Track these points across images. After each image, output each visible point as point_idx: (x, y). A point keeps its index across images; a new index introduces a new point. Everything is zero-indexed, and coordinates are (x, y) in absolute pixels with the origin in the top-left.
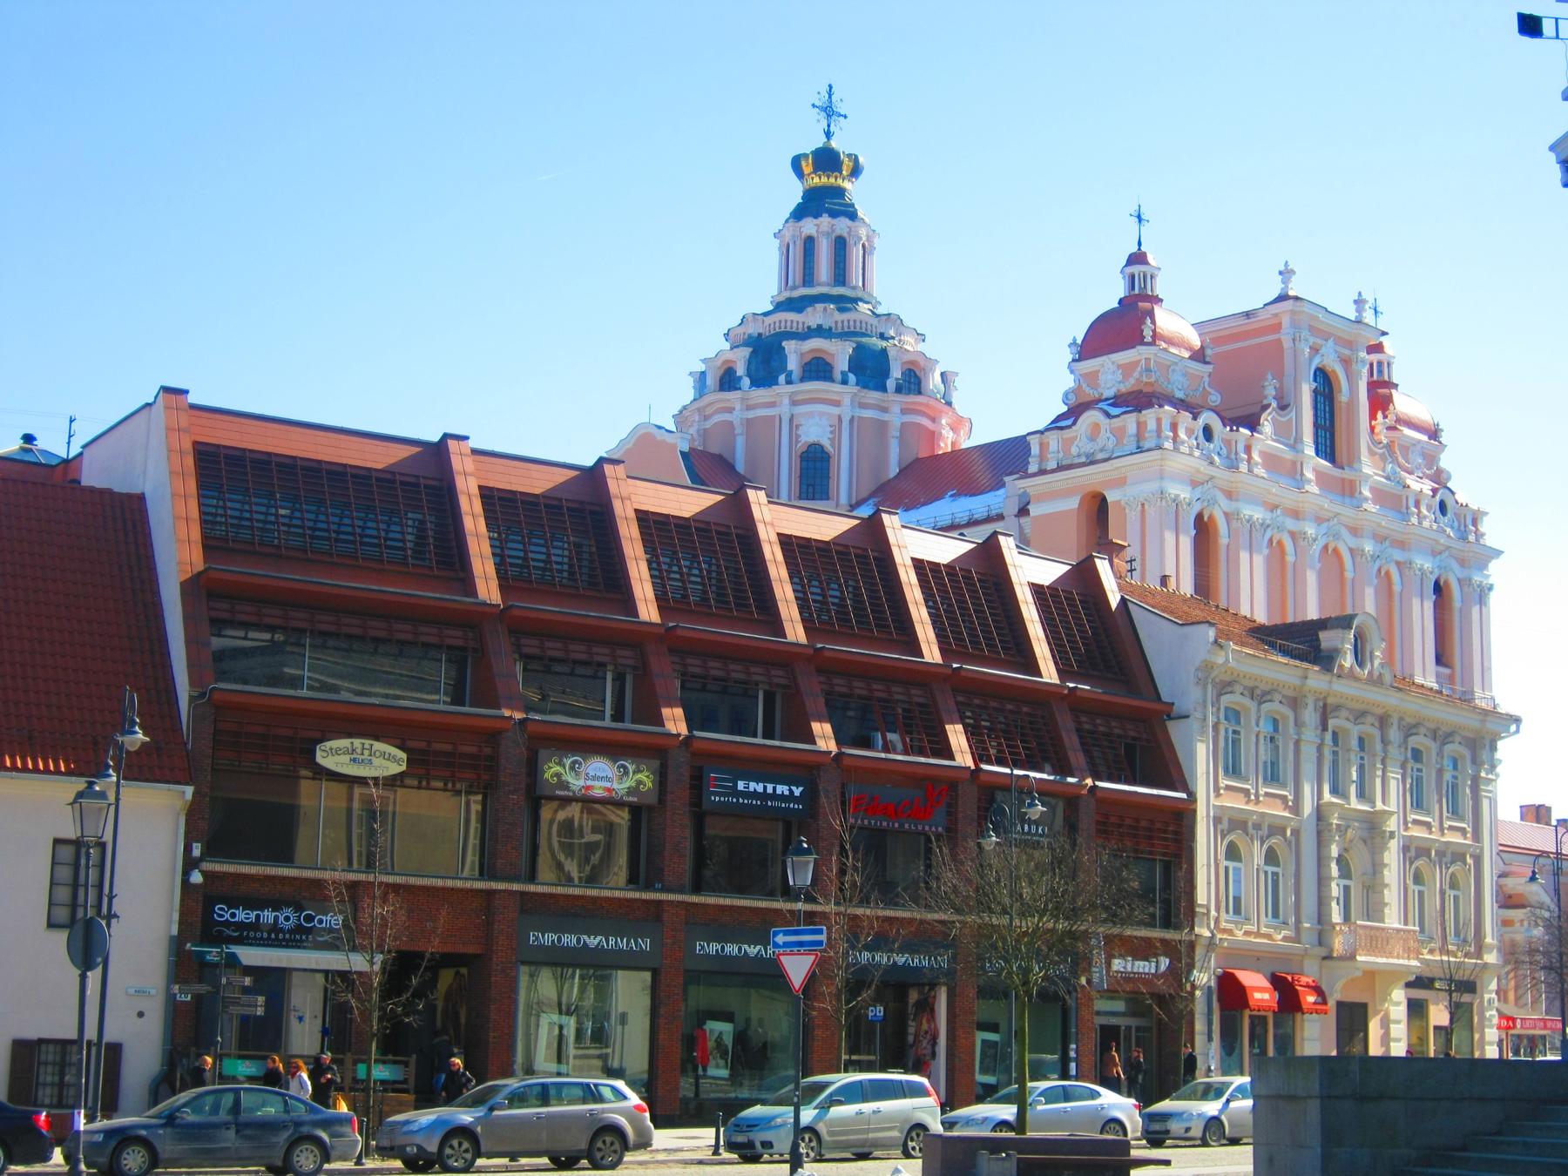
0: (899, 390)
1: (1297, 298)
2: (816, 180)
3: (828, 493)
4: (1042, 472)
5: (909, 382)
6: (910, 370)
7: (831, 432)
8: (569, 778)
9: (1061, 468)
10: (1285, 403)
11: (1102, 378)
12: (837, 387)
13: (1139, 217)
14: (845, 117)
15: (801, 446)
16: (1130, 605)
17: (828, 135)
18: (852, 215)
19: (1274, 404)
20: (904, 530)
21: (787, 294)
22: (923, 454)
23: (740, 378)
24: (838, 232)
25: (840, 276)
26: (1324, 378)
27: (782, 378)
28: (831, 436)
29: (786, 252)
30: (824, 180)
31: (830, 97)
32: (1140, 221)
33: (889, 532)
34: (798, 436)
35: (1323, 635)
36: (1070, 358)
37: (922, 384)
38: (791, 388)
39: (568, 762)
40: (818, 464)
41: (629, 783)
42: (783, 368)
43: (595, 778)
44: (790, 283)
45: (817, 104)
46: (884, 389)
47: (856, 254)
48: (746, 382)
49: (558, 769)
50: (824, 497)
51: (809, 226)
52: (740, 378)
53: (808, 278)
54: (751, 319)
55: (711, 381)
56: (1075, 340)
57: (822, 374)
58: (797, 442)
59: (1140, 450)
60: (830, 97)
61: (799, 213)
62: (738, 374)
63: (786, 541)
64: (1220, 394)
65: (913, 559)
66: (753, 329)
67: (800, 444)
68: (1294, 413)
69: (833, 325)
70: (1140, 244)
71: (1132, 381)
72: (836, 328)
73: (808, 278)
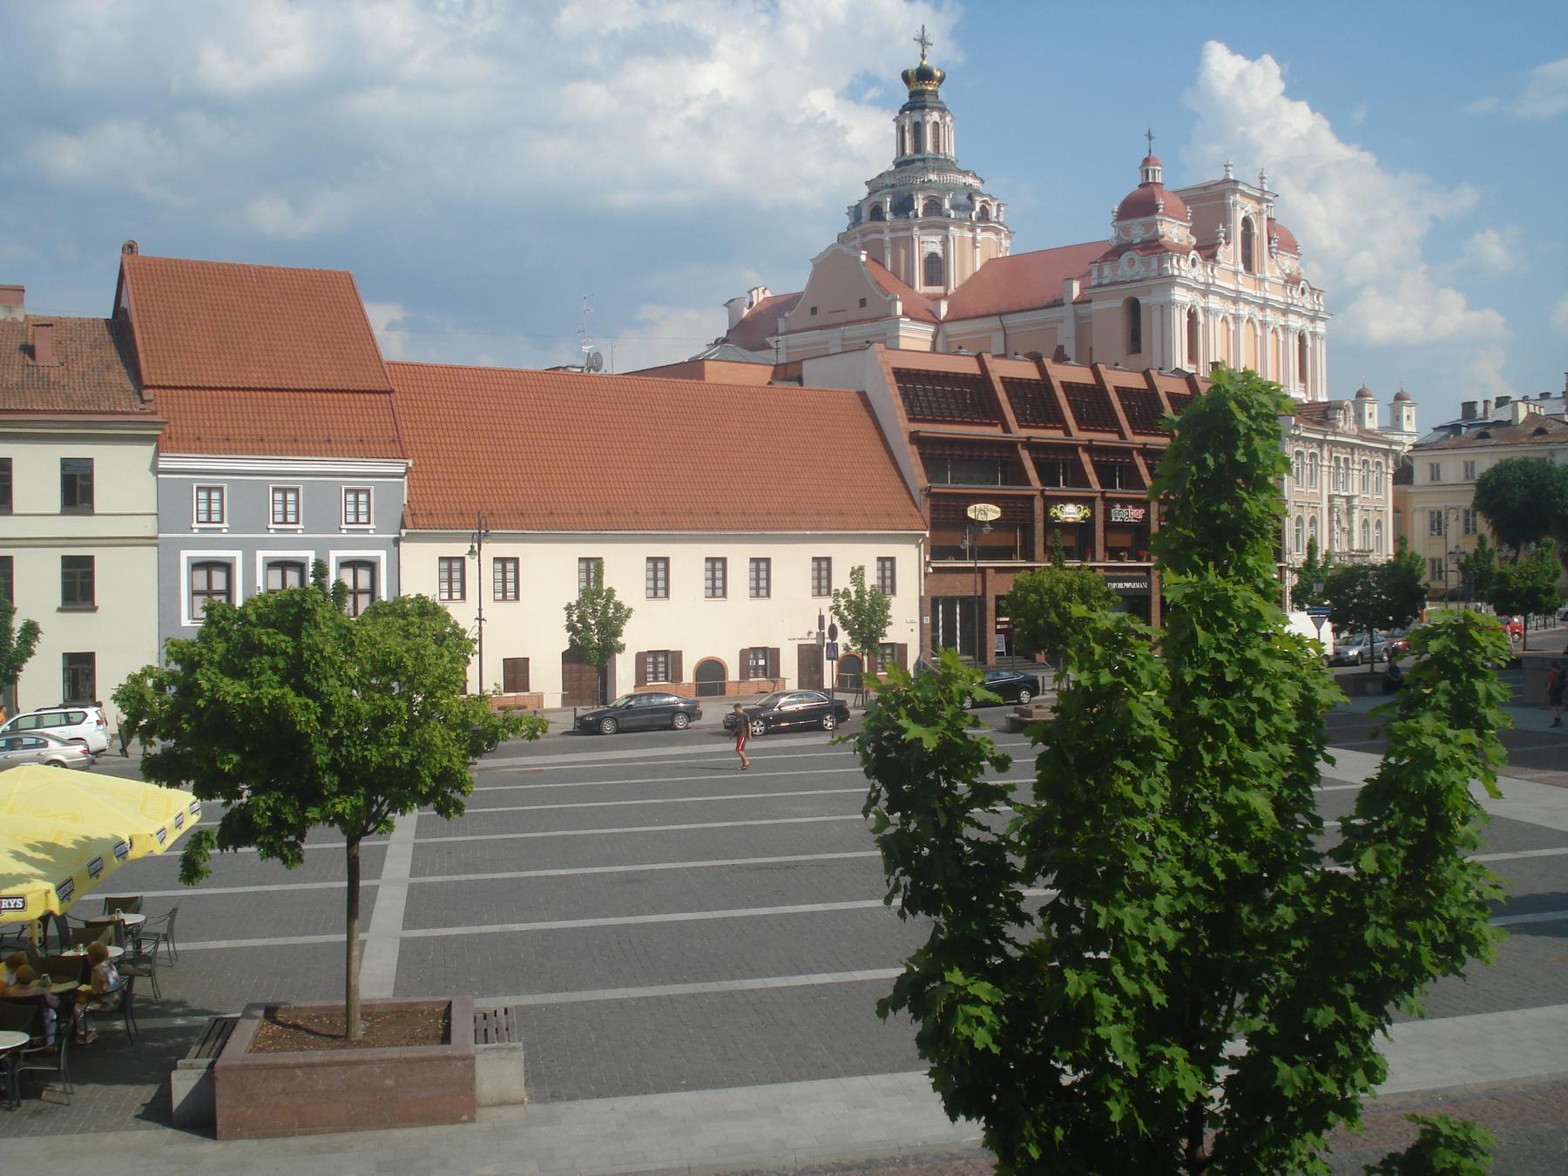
0: (979, 219)
4: (1100, 285)
8: (1059, 514)
9: (1112, 284)
11: (1133, 232)
12: (948, 220)
15: (925, 254)
17: (923, 57)
19: (1224, 242)
21: (903, 158)
22: (993, 256)
24: (934, 120)
26: (1246, 222)
29: (901, 130)
39: (1059, 507)
44: (908, 151)
46: (971, 216)
51: (917, 117)
53: (918, 145)
55: (865, 214)
71: (1151, 233)
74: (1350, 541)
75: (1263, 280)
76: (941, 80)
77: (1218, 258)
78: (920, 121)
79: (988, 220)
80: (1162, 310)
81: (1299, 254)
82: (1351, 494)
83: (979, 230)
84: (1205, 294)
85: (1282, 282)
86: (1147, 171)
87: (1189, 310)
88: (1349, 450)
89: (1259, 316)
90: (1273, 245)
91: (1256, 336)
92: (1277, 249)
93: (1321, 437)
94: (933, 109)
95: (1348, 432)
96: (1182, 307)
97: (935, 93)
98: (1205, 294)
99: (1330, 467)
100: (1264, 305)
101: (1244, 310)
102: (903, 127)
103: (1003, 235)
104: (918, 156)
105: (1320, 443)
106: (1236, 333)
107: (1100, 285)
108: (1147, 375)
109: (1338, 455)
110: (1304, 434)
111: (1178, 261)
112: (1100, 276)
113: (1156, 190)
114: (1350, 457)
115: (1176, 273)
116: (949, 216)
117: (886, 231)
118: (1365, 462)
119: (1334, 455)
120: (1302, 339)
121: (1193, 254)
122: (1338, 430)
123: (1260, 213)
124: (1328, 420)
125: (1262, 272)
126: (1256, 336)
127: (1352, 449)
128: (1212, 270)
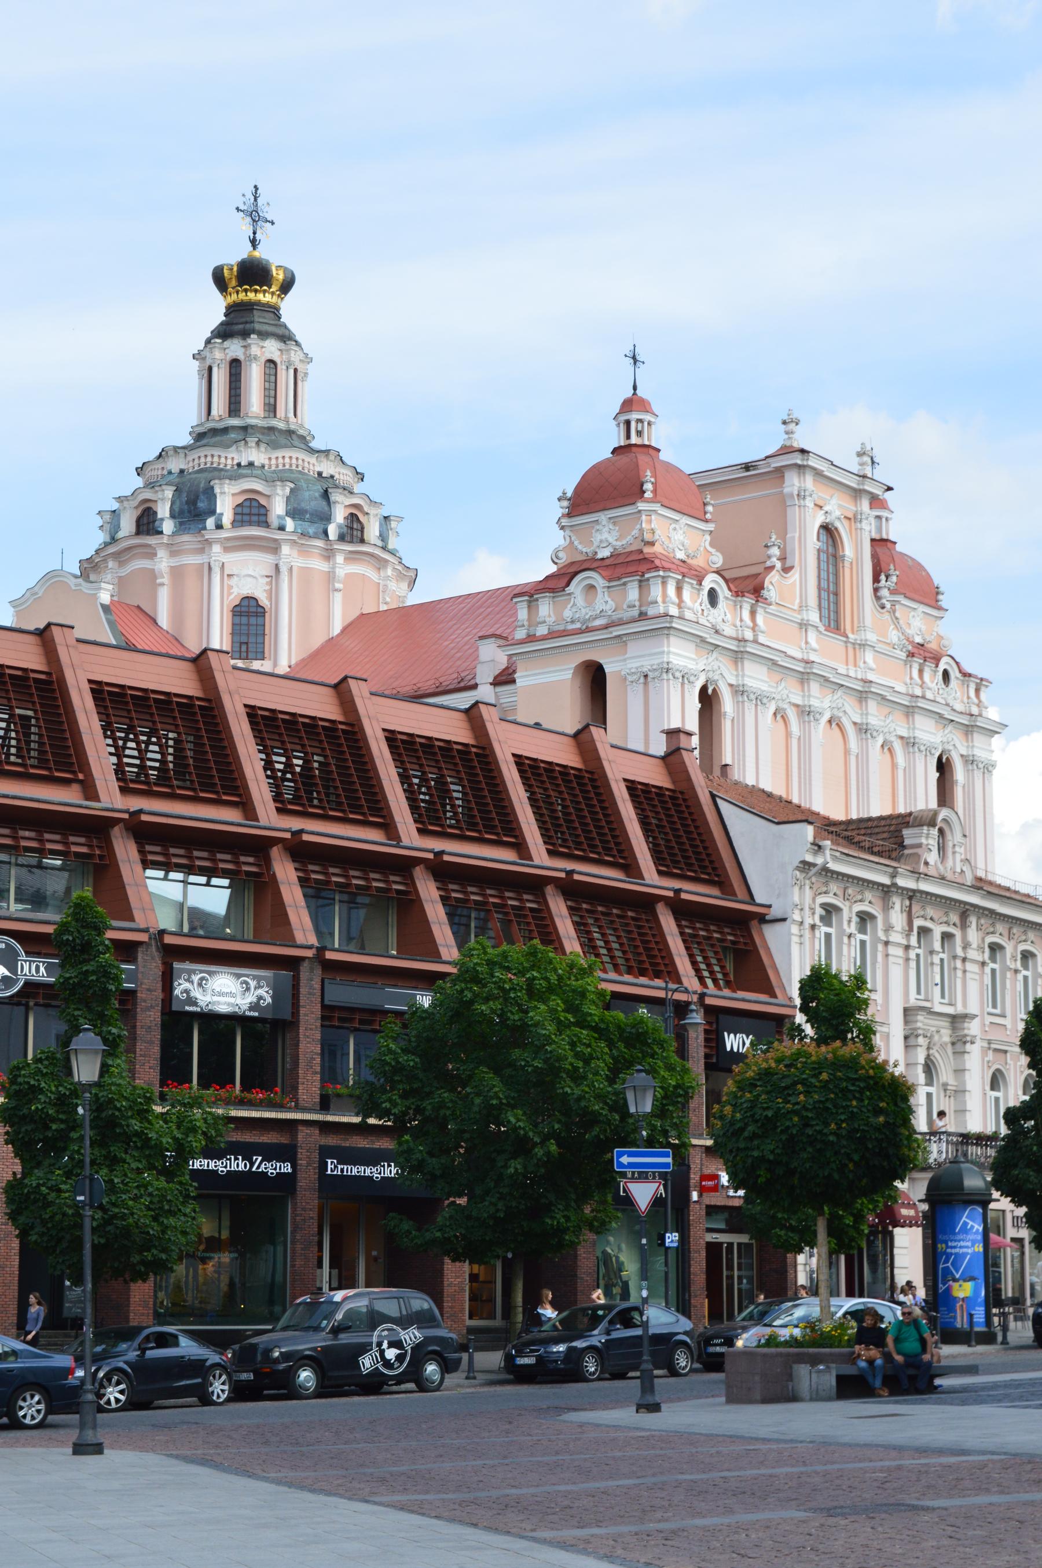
0: (342, 538)
1: (803, 451)
2: (242, 296)
3: (263, 652)
4: (531, 638)
5: (352, 528)
6: (352, 514)
7: (267, 583)
8: (196, 993)
10: (788, 564)
12: (278, 535)
13: (634, 358)
14: (273, 223)
15: (234, 599)
16: (719, 801)
17: (254, 243)
18: (286, 337)
19: (779, 565)
20: (374, 697)
21: (211, 425)
23: (162, 520)
25: (271, 408)
27: (210, 522)
28: (268, 588)
30: (251, 296)
31: (256, 199)
32: (635, 363)
33: (490, 727)
34: (230, 587)
35: (906, 832)
36: (560, 512)
37: (365, 530)
38: (223, 534)
39: (196, 978)
40: (253, 620)
41: (251, 998)
42: (213, 512)
43: (221, 994)
44: (214, 412)
45: (242, 207)
46: (326, 533)
47: (285, 378)
48: (168, 527)
49: (186, 985)
50: (259, 656)
51: (234, 348)
52: (162, 520)
53: (235, 405)
54: (171, 453)
55: (127, 525)
56: (564, 494)
57: (254, 518)
58: (230, 594)
59: (643, 616)
60: (256, 199)
61: (223, 333)
62: (159, 516)
63: (392, 738)
64: (723, 553)
65: (514, 755)
66: (175, 465)
67: (232, 597)
68: (797, 576)
69: (266, 462)
70: (635, 388)
72: (270, 466)
73: (235, 405)
74: (961, 1111)
75: (863, 645)
76: (286, 286)
77: (765, 593)
78: (241, 357)
79: (362, 541)
80: (646, 683)
81: (940, 608)
82: (960, 1009)
83: (340, 559)
84: (738, 656)
85: (903, 655)
86: (628, 423)
87: (704, 690)
88: (954, 918)
89: (852, 713)
90: (883, 582)
91: (847, 752)
92: (893, 592)
93: (886, 880)
94: (263, 335)
95: (949, 876)
96: (686, 678)
97: (274, 311)
98: (738, 656)
99: (907, 948)
100: (863, 694)
101: (820, 699)
102: (210, 369)
103: (389, 572)
104: (235, 422)
105: (886, 891)
106: (805, 743)
107: (531, 638)
108: (472, 714)
109: (928, 924)
110: (833, 866)
111: (679, 589)
112: (532, 622)
113: (642, 458)
114: (957, 932)
115: (674, 611)
116: (282, 528)
117: (161, 553)
118: (995, 948)
119: (918, 923)
120: (943, 767)
121: (711, 581)
122: (922, 869)
123: (854, 519)
124: (904, 847)
125: (860, 628)
126: (847, 752)
127: (964, 916)
128: (753, 613)
